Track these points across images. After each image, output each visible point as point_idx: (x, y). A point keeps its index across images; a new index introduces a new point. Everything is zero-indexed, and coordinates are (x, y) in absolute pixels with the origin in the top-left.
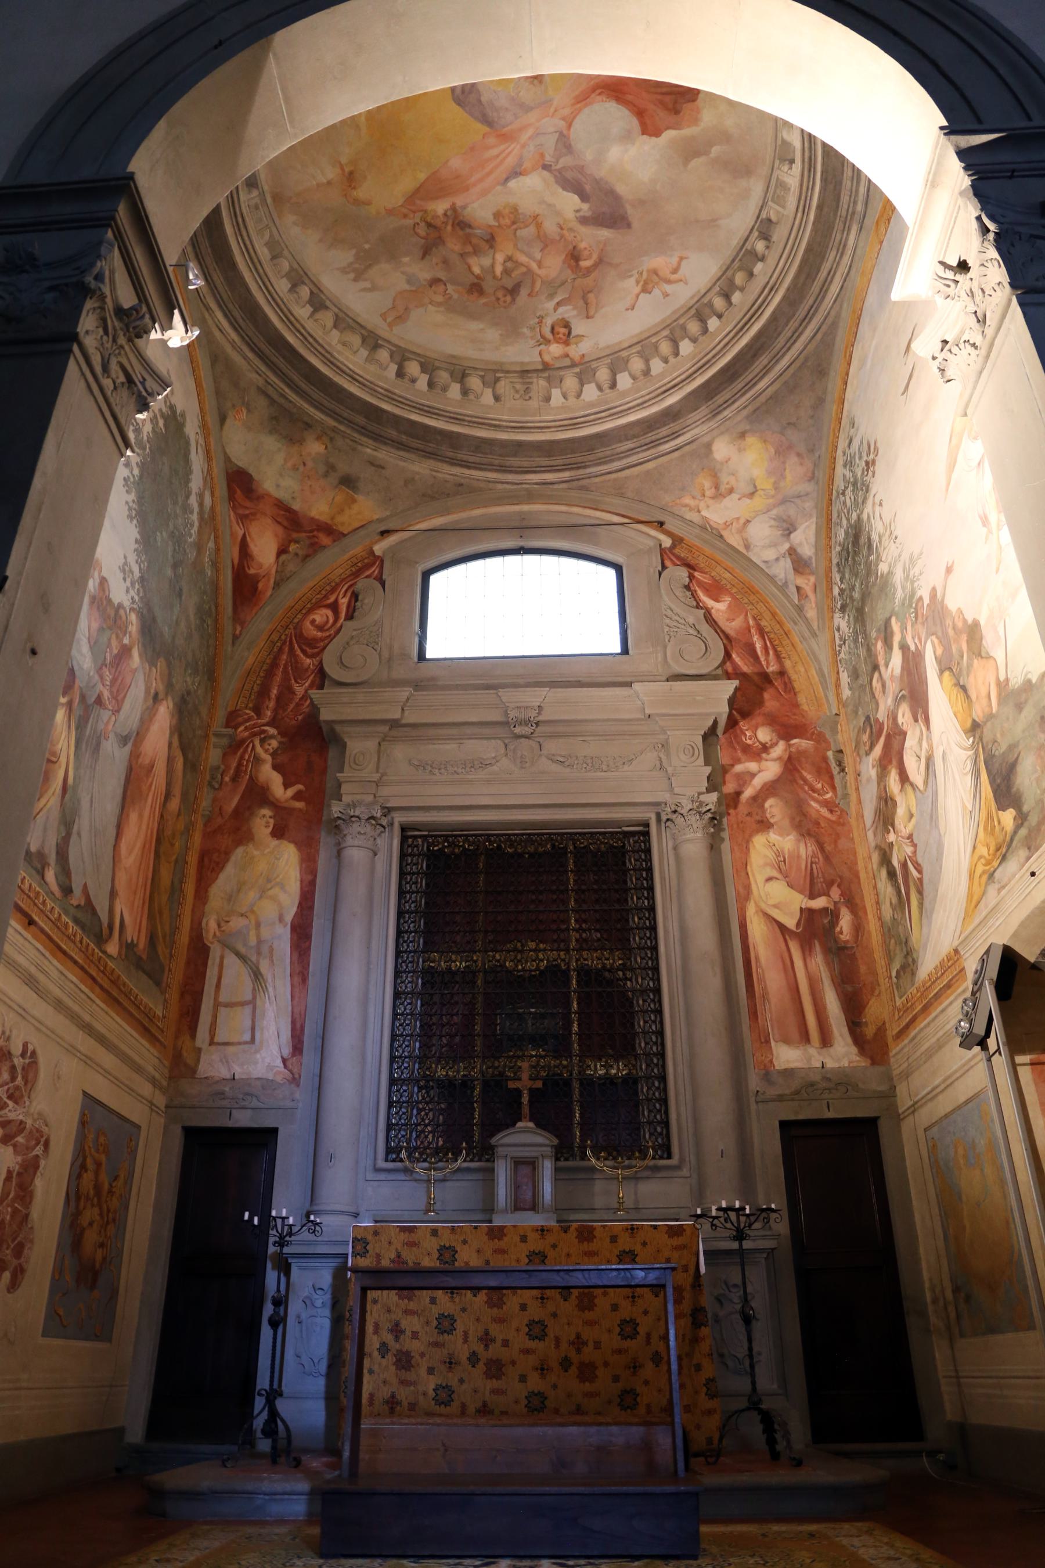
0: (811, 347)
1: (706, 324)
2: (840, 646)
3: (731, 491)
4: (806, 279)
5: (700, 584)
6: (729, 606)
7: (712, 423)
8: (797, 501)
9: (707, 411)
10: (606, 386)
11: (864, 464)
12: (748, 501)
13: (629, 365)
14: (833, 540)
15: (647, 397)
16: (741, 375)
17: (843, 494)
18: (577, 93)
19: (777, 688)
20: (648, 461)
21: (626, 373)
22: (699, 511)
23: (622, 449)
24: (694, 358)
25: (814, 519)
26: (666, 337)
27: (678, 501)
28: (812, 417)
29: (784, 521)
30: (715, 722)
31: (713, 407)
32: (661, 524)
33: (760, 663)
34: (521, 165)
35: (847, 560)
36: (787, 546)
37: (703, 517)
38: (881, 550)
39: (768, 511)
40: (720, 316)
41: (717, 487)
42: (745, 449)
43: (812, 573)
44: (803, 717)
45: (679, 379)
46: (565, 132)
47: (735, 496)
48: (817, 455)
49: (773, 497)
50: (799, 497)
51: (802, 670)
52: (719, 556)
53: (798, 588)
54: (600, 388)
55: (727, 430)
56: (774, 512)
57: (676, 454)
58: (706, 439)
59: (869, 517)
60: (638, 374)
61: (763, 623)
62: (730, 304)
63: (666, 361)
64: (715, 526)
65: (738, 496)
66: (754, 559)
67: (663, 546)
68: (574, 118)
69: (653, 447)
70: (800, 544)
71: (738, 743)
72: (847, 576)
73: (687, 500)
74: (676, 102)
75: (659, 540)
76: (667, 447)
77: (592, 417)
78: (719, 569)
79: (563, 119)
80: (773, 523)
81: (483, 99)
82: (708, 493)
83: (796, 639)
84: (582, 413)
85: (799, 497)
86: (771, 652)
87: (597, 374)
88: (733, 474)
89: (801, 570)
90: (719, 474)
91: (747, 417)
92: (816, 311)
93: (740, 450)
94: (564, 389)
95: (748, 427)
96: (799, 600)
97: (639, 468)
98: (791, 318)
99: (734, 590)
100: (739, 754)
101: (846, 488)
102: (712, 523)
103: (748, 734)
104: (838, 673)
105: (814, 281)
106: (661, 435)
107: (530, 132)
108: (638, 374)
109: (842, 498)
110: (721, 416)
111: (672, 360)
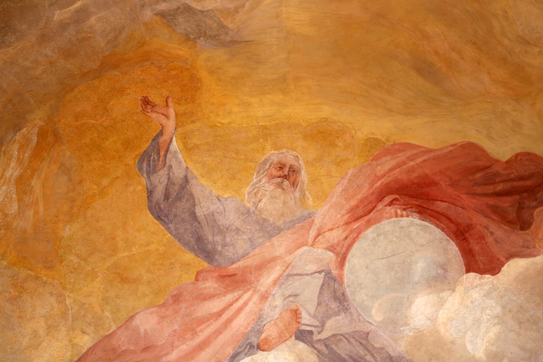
18: (353, 203)
34: (260, 332)
46: (335, 272)
68: (350, 246)
74: (521, 208)
79: (331, 248)
81: (200, 212)
107: (276, 271)
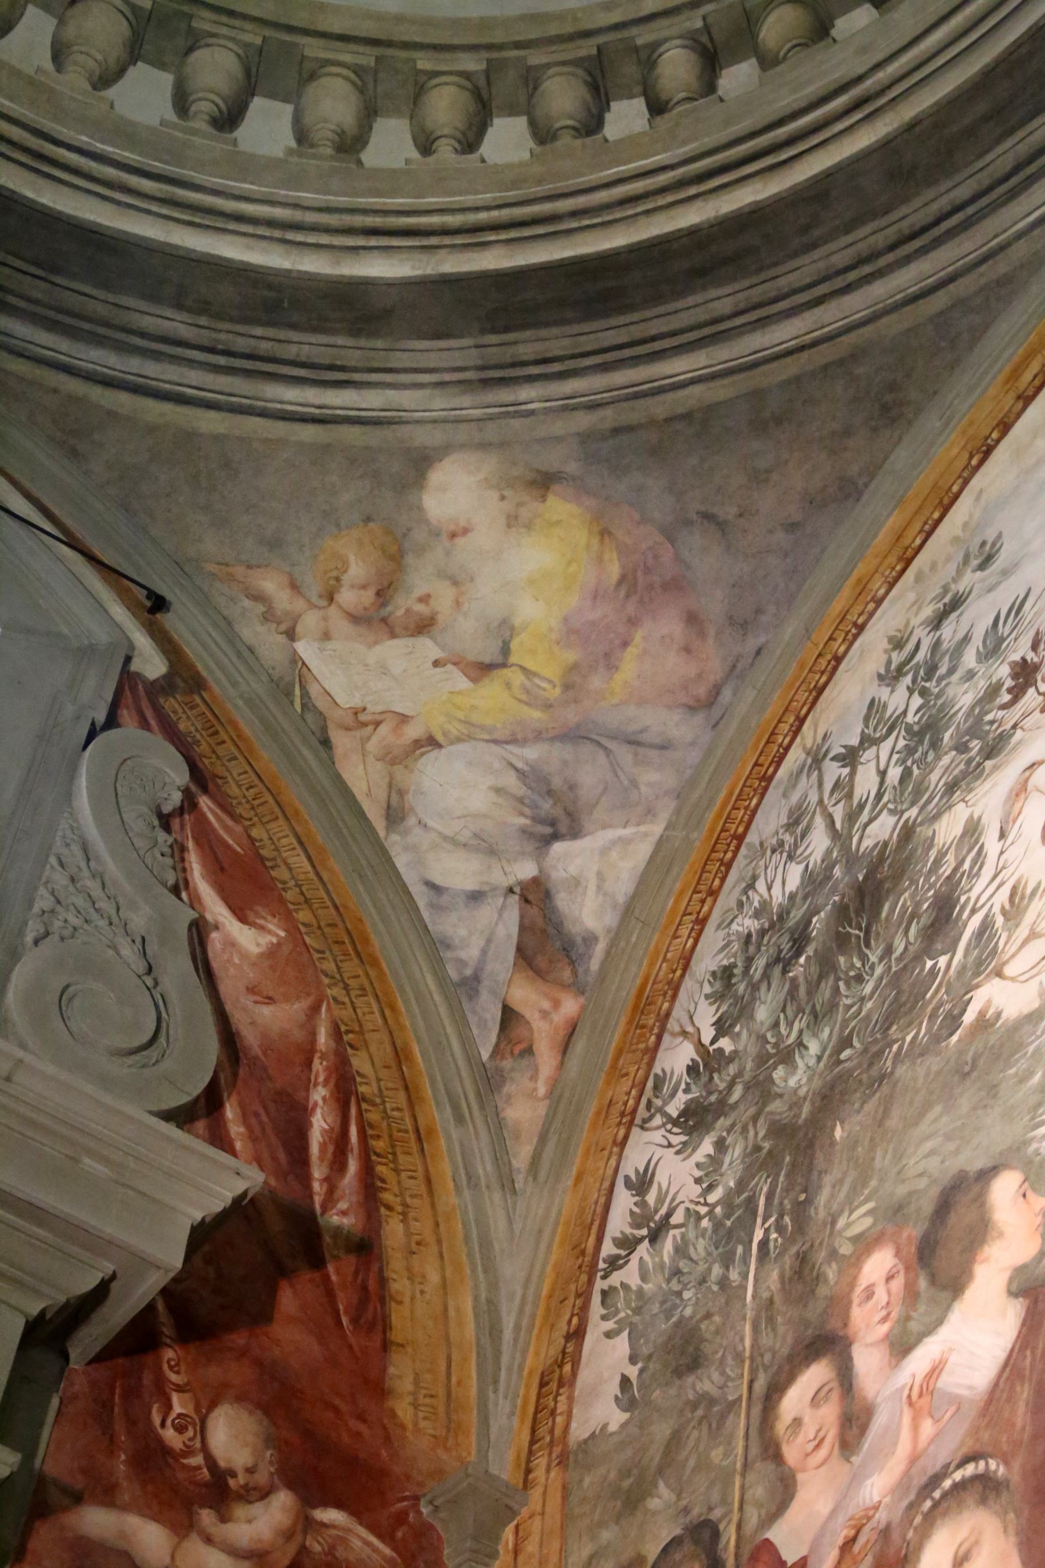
0: (892, 326)
1: (604, 107)
2: (628, 1244)
3: (423, 626)
4: (986, 118)
5: (205, 837)
6: (272, 952)
7: (466, 400)
8: (624, 754)
9: (472, 357)
10: (203, 107)
11: (1003, 671)
12: (462, 683)
13: (311, 90)
14: (728, 898)
15: (311, 217)
16: (631, 308)
17: (850, 757)
19: (330, 1294)
20: (210, 405)
21: (289, 108)
22: (291, 635)
23: (148, 323)
24: (515, 184)
25: (657, 829)
26: (466, 75)
27: (239, 571)
28: (792, 527)
29: (550, 793)
30: (101, 1292)
31: (494, 354)
32: (158, 604)
33: (306, 1180)
35: (783, 962)
36: (526, 870)
37: (295, 659)
38: (1006, 942)
39: (513, 741)
40: (657, 108)
41: (383, 594)
42: (529, 526)
43: (578, 988)
44: (387, 1439)
45: (435, 220)
47: (428, 648)
48: (752, 643)
49: (548, 706)
50: (633, 742)
51: (434, 1278)
52: (295, 793)
53: (509, 1016)
54: (182, 102)
55: (503, 445)
56: (531, 753)
57: (308, 433)
58: (423, 437)
59: (973, 830)
60: (323, 134)
61: (359, 1062)
62: (710, 88)
63: (426, 145)
64: (321, 703)
65: (436, 653)
66: (401, 861)
67: (134, 667)
69: (248, 373)
70: (576, 883)
71: (131, 1422)
72: (762, 1014)
73: (271, 584)
75: (132, 646)
76: (291, 396)
77: (110, 172)
78: (280, 827)
80: (511, 781)
82: (347, 597)
83: (445, 1169)
84: (83, 140)
85: (633, 742)
86: (353, 1166)
87: (200, 56)
88: (456, 583)
89: (541, 961)
90: (410, 560)
91: (586, 438)
92: (966, 226)
93: (512, 521)
94: (70, 32)
95: (572, 467)
96: (497, 1052)
97: (167, 407)
98: (874, 215)
99: (303, 916)
100: (121, 1465)
101: (867, 741)
102: (314, 690)
103: (179, 1405)
104: (577, 1335)
105: (999, 140)
106: (291, 351)
108: (323, 134)
109: (833, 771)
110: (506, 395)
111: (445, 152)
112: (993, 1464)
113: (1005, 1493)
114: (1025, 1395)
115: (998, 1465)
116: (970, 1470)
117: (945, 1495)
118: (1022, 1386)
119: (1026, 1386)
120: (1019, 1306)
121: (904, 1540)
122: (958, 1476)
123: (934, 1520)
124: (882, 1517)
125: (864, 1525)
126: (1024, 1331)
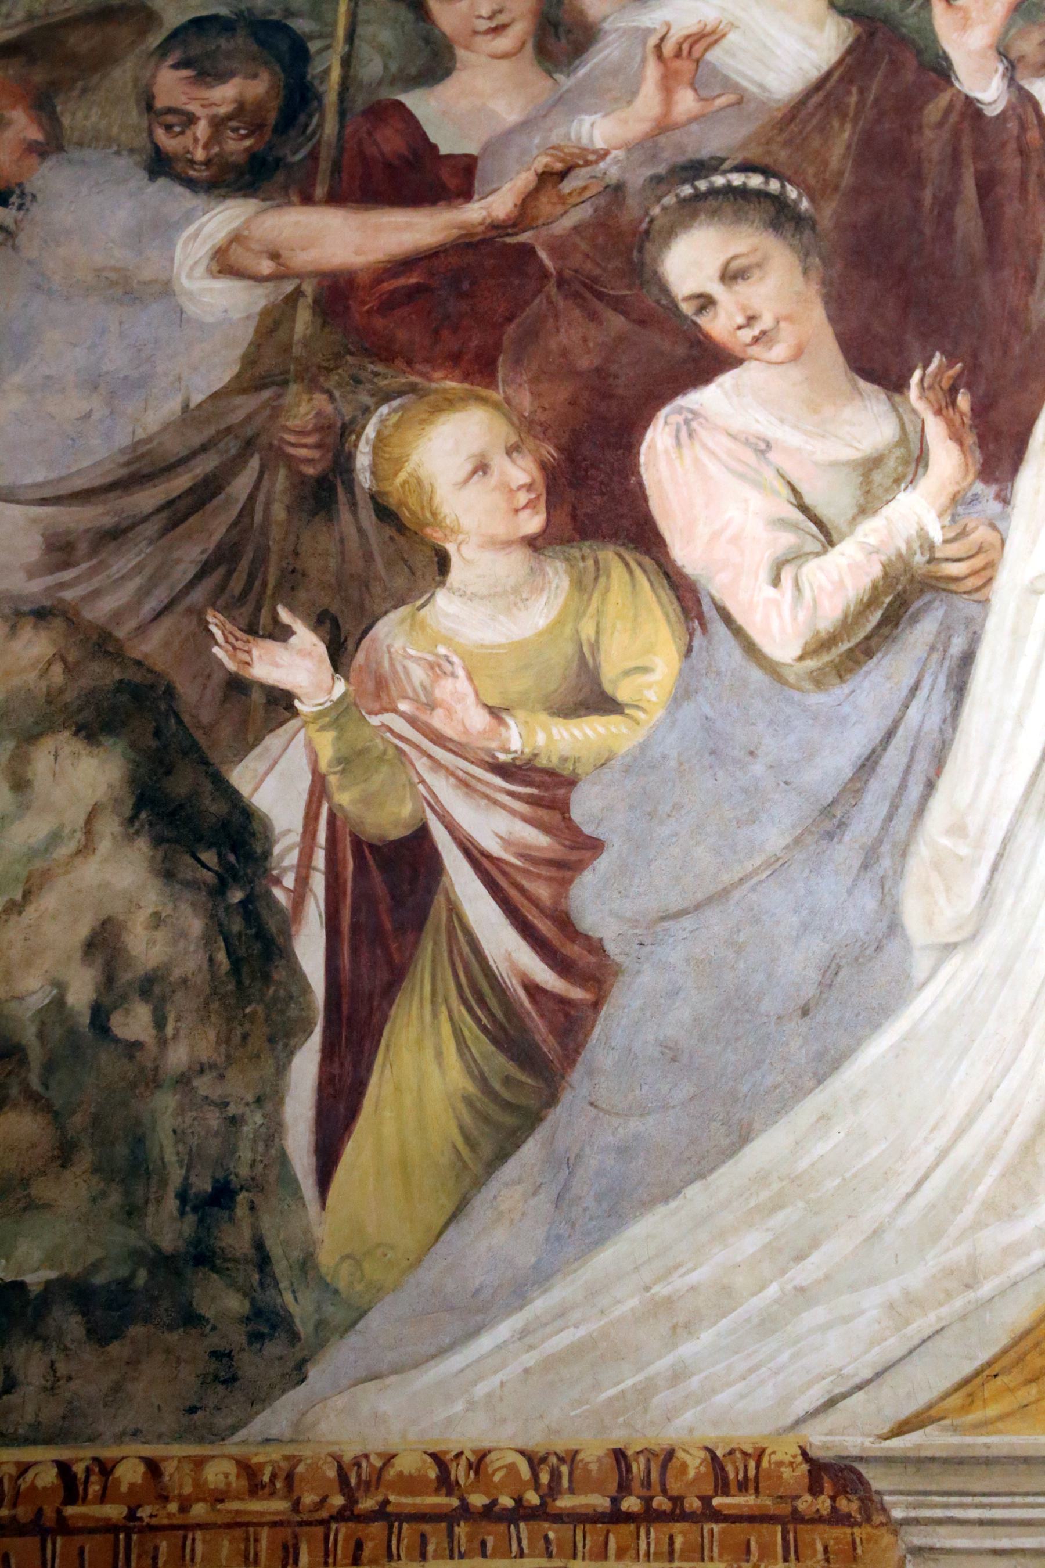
112: (792, 193)
113: (807, 233)
114: (846, 135)
115: (800, 195)
116: (755, 181)
117: (714, 192)
118: (842, 124)
119: (848, 126)
120: (844, 28)
121: (647, 214)
122: (737, 179)
123: (694, 215)
124: (611, 169)
125: (578, 166)
126: (849, 60)
